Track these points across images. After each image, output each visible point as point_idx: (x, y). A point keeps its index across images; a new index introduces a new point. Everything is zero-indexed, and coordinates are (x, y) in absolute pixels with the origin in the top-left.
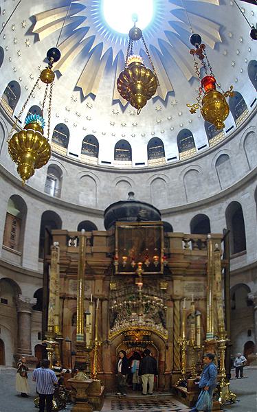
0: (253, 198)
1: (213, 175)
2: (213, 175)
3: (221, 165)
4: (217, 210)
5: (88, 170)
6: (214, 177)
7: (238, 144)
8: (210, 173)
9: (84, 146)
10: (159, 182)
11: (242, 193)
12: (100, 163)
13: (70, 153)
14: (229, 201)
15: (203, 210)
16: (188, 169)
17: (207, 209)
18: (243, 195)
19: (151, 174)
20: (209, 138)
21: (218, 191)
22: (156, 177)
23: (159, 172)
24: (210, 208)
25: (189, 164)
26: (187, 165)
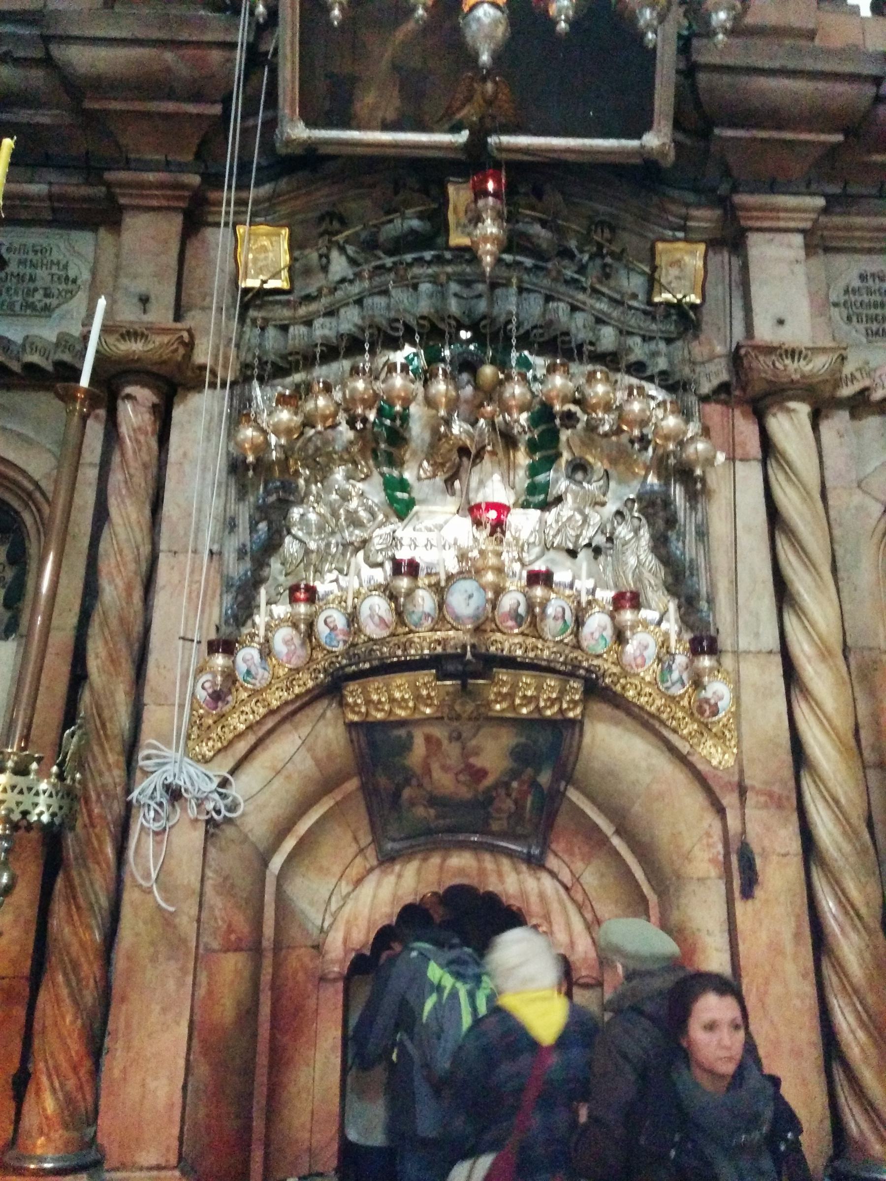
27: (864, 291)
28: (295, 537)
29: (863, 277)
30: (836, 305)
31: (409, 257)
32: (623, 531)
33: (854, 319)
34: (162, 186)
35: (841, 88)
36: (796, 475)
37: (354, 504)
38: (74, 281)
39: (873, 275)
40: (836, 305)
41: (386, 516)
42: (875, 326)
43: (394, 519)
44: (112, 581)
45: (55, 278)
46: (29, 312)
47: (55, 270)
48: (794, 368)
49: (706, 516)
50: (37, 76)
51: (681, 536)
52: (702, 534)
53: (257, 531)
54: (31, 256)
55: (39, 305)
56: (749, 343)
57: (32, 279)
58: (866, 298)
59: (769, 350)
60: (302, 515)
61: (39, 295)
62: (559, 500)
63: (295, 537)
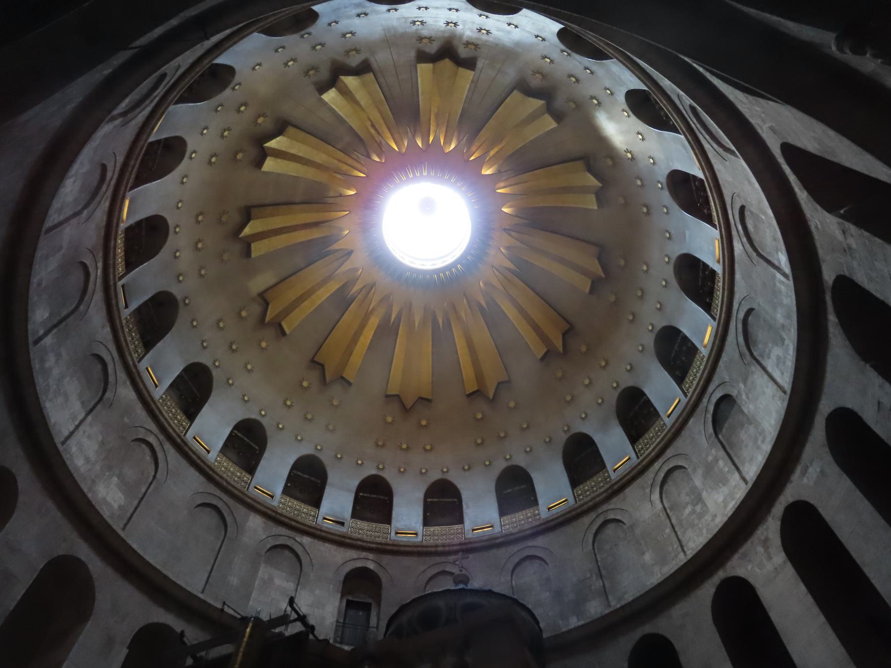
0: (834, 470)
2: (716, 460)
3: (726, 425)
4: (760, 549)
5: (443, 559)
6: (721, 463)
7: (737, 355)
8: (710, 458)
10: (610, 530)
11: (798, 470)
12: (469, 535)
14: (778, 509)
15: (729, 565)
16: (662, 475)
17: (736, 556)
18: (804, 472)
19: (586, 520)
21: (741, 492)
22: (599, 521)
23: (605, 507)
24: (741, 551)
25: (661, 461)
26: (657, 465)
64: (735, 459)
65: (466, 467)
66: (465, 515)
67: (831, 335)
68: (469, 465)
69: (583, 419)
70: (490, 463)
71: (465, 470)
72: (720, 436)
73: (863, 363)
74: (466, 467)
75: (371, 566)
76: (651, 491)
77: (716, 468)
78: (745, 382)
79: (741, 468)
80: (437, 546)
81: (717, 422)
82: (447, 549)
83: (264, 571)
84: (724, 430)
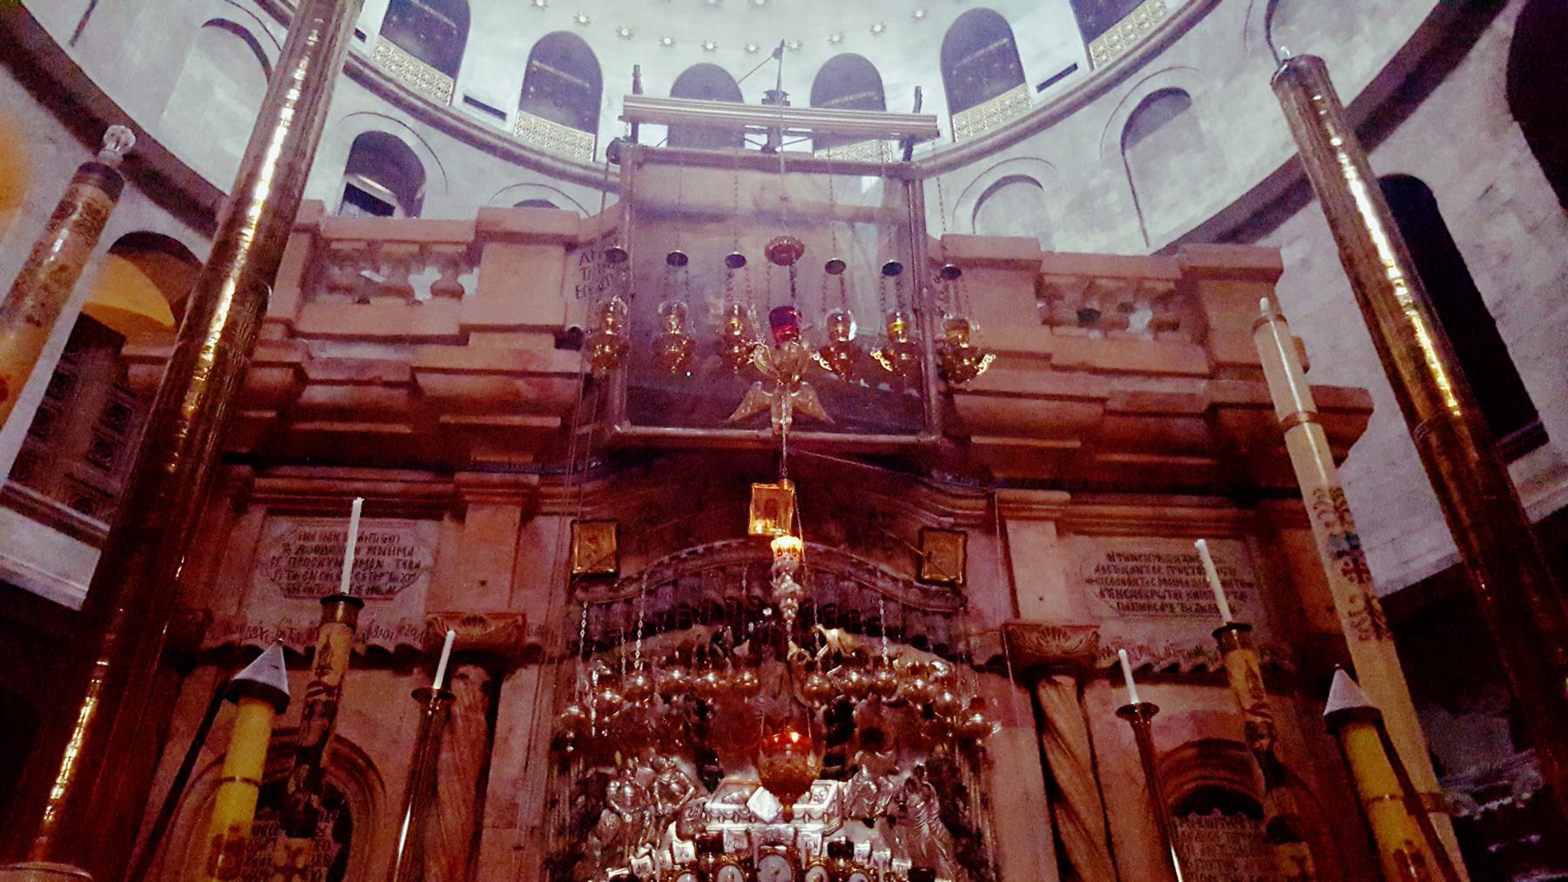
1: (1106, 188)
2: (1106, 188)
6: (1113, 196)
8: (1095, 182)
9: (531, 77)
13: (467, 99)
16: (989, 182)
20: (1090, 33)
25: (997, 157)
26: (985, 163)
27: (1112, 569)
28: (612, 810)
29: (1110, 557)
30: (1090, 581)
31: (718, 544)
32: (916, 800)
33: (1106, 594)
34: (502, 485)
35: (1077, 406)
36: (1063, 741)
37: (666, 778)
38: (418, 566)
39: (1119, 555)
40: (1090, 581)
41: (696, 788)
42: (1125, 601)
43: (704, 790)
44: (438, 860)
45: (401, 564)
46: (374, 596)
47: (401, 556)
48: (1054, 646)
49: (988, 783)
50: (400, 394)
51: (967, 801)
52: (986, 802)
53: (576, 805)
54: (380, 544)
55: (385, 589)
56: (1017, 621)
57: (380, 564)
58: (1115, 576)
59: (1035, 627)
60: (619, 788)
61: (385, 579)
62: (856, 769)
63: (612, 810)
64: (1141, 198)
65: (625, 32)
66: (602, 119)
67: (1474, 53)
68: (630, 30)
69: (875, 33)
70: (673, 43)
71: (620, 35)
72: (1128, 153)
73: (1510, 117)
74: (625, 32)
75: (409, 140)
76: (959, 201)
77: (1099, 201)
78: (1229, 79)
79: (1145, 215)
80: (543, 154)
81: (1132, 129)
82: (560, 165)
83: (196, 65)
84: (1140, 146)
